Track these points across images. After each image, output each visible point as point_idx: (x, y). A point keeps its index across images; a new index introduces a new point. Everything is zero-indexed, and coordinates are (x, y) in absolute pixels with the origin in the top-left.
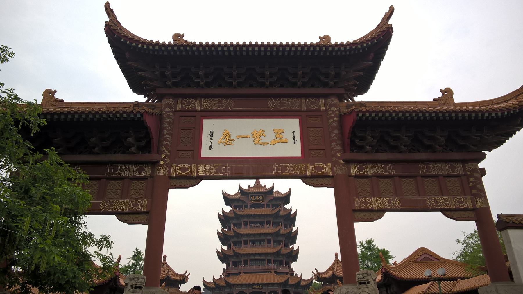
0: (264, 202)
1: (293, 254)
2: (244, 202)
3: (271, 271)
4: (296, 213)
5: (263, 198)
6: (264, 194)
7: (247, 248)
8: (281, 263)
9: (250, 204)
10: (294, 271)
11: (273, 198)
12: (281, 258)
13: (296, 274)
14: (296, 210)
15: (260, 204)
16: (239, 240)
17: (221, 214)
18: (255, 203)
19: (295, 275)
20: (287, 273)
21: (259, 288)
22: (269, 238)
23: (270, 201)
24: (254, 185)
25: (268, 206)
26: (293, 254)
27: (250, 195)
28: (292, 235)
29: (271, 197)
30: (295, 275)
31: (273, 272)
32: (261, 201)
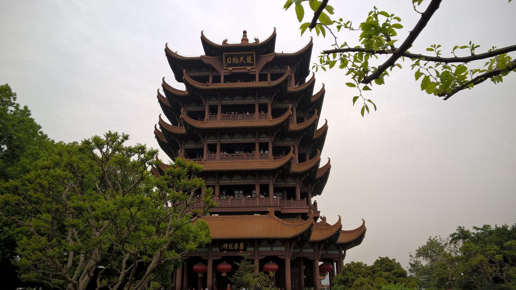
0: (252, 70)
1: (318, 175)
2: (213, 69)
3: (268, 209)
4: (322, 93)
5: (252, 60)
6: (254, 53)
7: (214, 159)
8: (290, 194)
10: (319, 212)
11: (273, 57)
12: (290, 183)
13: (324, 219)
16: (198, 146)
17: (163, 94)
19: (321, 220)
20: (304, 216)
21: (239, 250)
22: (264, 139)
23: (266, 67)
25: (263, 78)
26: (318, 175)
27: (224, 54)
28: (315, 137)
29: (269, 58)
30: (319, 220)
32: (249, 68)
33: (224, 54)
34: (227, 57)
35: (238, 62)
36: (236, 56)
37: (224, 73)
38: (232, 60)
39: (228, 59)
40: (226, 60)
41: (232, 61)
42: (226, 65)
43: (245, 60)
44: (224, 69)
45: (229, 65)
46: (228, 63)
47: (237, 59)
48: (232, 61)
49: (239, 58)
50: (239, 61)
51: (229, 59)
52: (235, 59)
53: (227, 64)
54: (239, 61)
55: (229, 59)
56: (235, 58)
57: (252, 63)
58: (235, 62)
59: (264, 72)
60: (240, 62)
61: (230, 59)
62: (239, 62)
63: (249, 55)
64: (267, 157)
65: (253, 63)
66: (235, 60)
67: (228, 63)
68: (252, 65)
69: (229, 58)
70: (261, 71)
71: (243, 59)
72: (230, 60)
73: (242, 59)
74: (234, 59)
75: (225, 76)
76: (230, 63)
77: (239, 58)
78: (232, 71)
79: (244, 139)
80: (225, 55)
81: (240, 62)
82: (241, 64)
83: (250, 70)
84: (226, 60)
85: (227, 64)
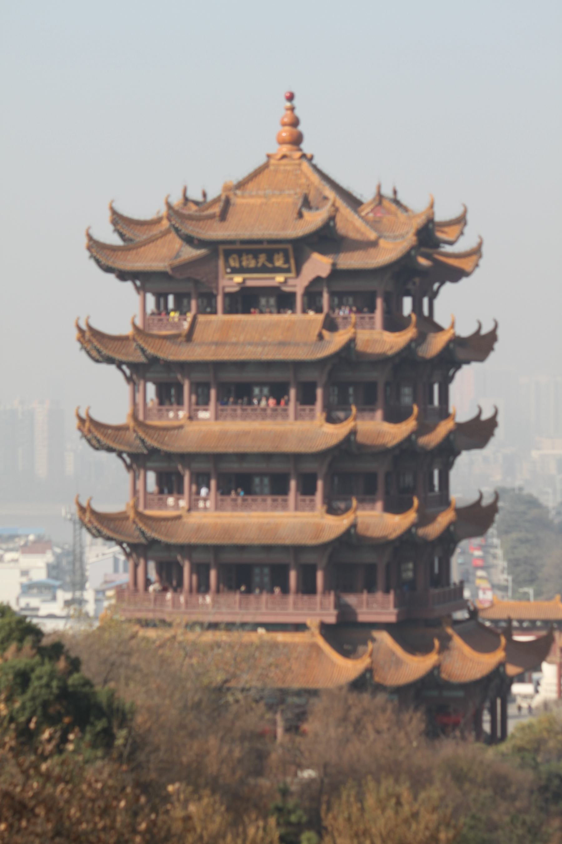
5: (287, 261)
6: (289, 247)
9: (228, 290)
15: (275, 291)
18: (249, 283)
24: (269, 156)
27: (221, 248)
31: (316, 631)
32: (280, 278)
36: (248, 252)
41: (240, 262)
43: (270, 259)
45: (235, 271)
48: (240, 262)
50: (257, 262)
63: (278, 251)
64: (312, 508)
68: (288, 271)
73: (262, 258)
74: (244, 258)
77: (256, 257)
82: (263, 269)
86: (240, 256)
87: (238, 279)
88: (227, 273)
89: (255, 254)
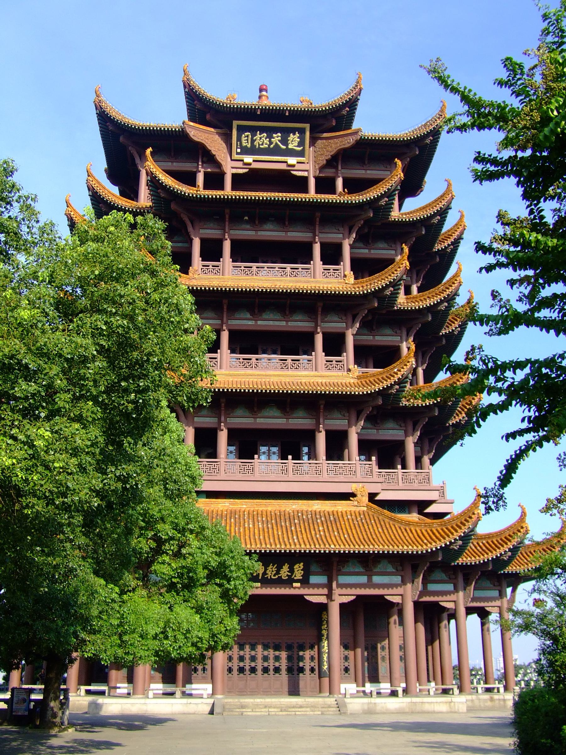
6: (307, 126)
9: (235, 171)
14: (462, 216)
27: (235, 123)
32: (292, 161)
33: (235, 123)
34: (242, 130)
35: (267, 146)
36: (262, 130)
37: (232, 168)
38: (255, 138)
39: (245, 137)
40: (239, 139)
41: (253, 141)
42: (239, 150)
43: (285, 141)
44: (232, 160)
45: (245, 151)
46: (244, 144)
47: (266, 139)
48: (253, 141)
49: (270, 137)
50: (271, 143)
51: (248, 136)
52: (261, 138)
53: (242, 147)
54: (271, 143)
55: (248, 136)
56: (262, 135)
57: (298, 151)
58: (259, 145)
59: (329, 173)
60: (272, 146)
61: (250, 136)
62: (269, 146)
65: (303, 149)
66: (262, 140)
67: (244, 144)
68: (301, 154)
69: (246, 134)
70: (322, 169)
71: (280, 138)
72: (247, 140)
74: (258, 136)
75: (234, 176)
76: (249, 146)
77: (270, 137)
78: (250, 164)
79: (287, 321)
80: (238, 126)
81: (272, 146)
82: (276, 151)
83: (294, 166)
84: (239, 139)
85: (242, 147)
86: (254, 135)
87: (248, 159)
88: (237, 153)
89: (270, 131)
